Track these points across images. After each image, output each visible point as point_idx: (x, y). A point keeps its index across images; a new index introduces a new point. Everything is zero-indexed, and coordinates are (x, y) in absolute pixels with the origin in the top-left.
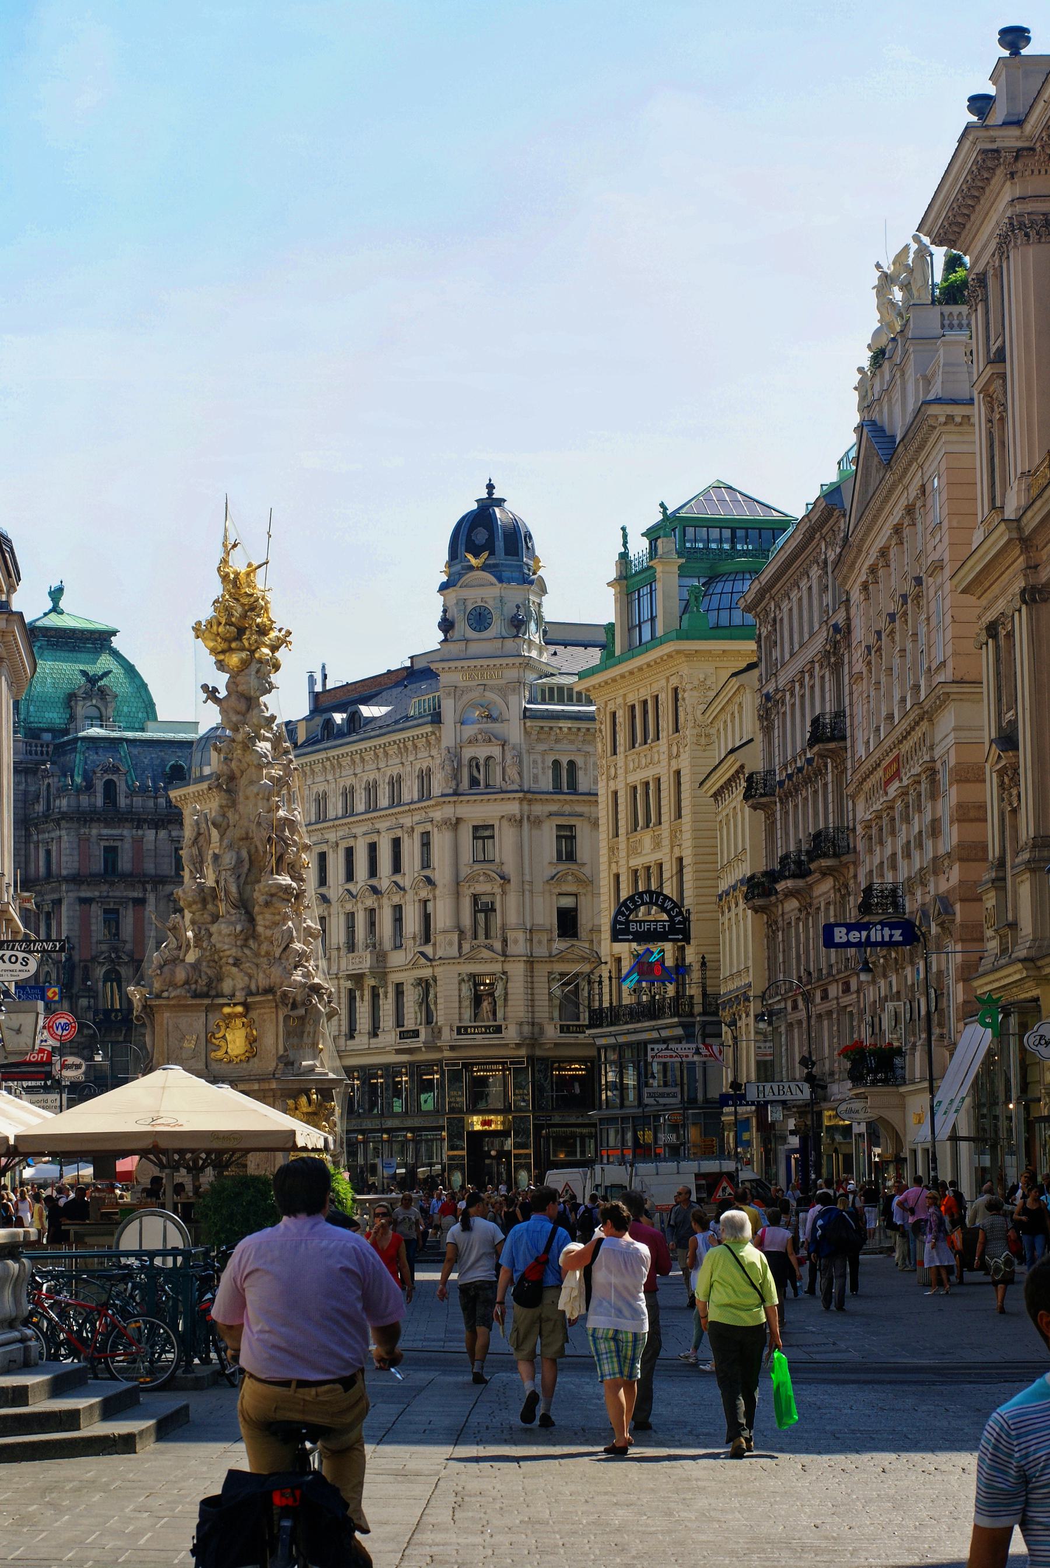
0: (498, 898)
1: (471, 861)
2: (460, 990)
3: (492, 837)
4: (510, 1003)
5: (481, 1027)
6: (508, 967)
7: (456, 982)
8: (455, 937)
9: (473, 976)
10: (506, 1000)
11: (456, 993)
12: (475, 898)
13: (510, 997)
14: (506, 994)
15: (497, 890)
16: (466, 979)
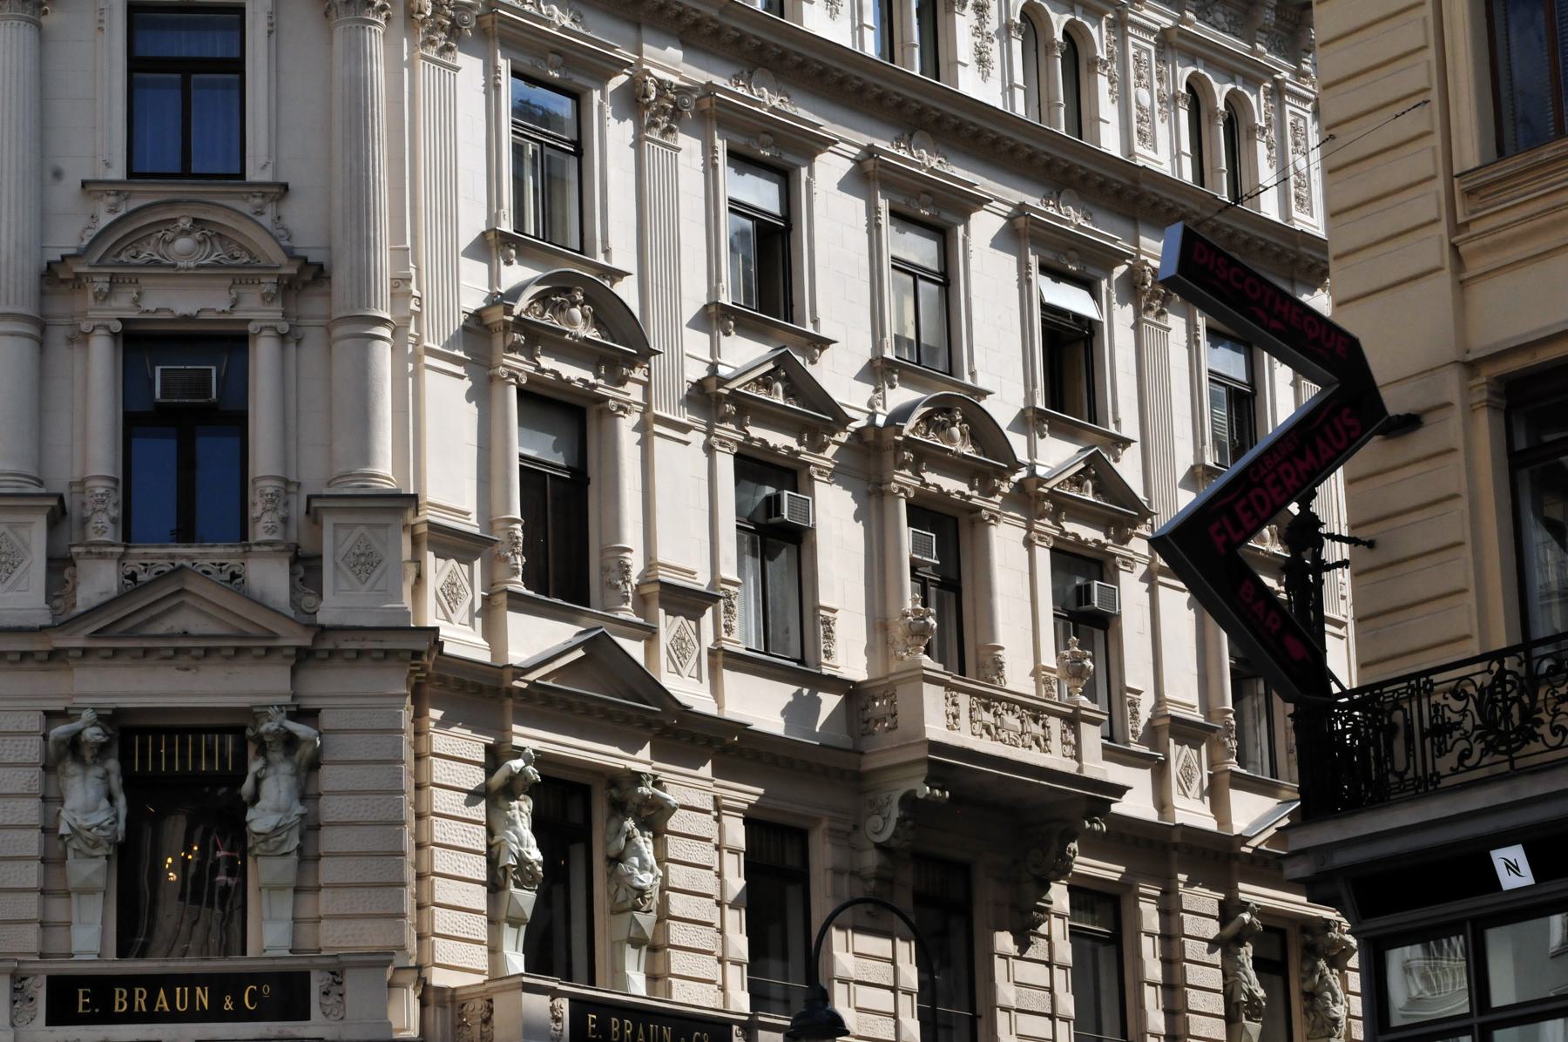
0: (263, 355)
1: (118, 172)
2: (51, 800)
3: (236, 66)
4: (329, 871)
5: (190, 980)
6: (323, 686)
7: (32, 750)
8: (36, 535)
9: (128, 733)
10: (307, 857)
11: (30, 811)
12: (136, 342)
13: (329, 840)
14: (310, 827)
15: (257, 309)
16: (93, 734)
